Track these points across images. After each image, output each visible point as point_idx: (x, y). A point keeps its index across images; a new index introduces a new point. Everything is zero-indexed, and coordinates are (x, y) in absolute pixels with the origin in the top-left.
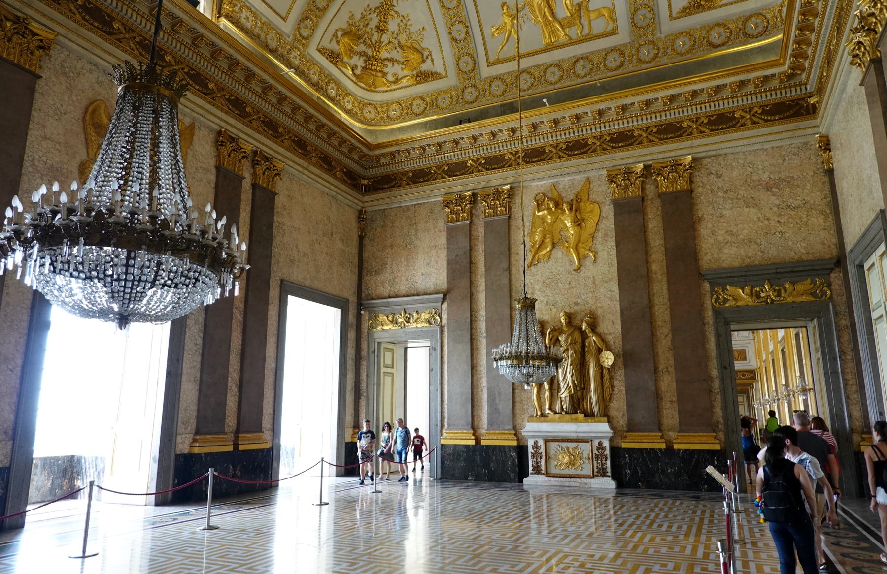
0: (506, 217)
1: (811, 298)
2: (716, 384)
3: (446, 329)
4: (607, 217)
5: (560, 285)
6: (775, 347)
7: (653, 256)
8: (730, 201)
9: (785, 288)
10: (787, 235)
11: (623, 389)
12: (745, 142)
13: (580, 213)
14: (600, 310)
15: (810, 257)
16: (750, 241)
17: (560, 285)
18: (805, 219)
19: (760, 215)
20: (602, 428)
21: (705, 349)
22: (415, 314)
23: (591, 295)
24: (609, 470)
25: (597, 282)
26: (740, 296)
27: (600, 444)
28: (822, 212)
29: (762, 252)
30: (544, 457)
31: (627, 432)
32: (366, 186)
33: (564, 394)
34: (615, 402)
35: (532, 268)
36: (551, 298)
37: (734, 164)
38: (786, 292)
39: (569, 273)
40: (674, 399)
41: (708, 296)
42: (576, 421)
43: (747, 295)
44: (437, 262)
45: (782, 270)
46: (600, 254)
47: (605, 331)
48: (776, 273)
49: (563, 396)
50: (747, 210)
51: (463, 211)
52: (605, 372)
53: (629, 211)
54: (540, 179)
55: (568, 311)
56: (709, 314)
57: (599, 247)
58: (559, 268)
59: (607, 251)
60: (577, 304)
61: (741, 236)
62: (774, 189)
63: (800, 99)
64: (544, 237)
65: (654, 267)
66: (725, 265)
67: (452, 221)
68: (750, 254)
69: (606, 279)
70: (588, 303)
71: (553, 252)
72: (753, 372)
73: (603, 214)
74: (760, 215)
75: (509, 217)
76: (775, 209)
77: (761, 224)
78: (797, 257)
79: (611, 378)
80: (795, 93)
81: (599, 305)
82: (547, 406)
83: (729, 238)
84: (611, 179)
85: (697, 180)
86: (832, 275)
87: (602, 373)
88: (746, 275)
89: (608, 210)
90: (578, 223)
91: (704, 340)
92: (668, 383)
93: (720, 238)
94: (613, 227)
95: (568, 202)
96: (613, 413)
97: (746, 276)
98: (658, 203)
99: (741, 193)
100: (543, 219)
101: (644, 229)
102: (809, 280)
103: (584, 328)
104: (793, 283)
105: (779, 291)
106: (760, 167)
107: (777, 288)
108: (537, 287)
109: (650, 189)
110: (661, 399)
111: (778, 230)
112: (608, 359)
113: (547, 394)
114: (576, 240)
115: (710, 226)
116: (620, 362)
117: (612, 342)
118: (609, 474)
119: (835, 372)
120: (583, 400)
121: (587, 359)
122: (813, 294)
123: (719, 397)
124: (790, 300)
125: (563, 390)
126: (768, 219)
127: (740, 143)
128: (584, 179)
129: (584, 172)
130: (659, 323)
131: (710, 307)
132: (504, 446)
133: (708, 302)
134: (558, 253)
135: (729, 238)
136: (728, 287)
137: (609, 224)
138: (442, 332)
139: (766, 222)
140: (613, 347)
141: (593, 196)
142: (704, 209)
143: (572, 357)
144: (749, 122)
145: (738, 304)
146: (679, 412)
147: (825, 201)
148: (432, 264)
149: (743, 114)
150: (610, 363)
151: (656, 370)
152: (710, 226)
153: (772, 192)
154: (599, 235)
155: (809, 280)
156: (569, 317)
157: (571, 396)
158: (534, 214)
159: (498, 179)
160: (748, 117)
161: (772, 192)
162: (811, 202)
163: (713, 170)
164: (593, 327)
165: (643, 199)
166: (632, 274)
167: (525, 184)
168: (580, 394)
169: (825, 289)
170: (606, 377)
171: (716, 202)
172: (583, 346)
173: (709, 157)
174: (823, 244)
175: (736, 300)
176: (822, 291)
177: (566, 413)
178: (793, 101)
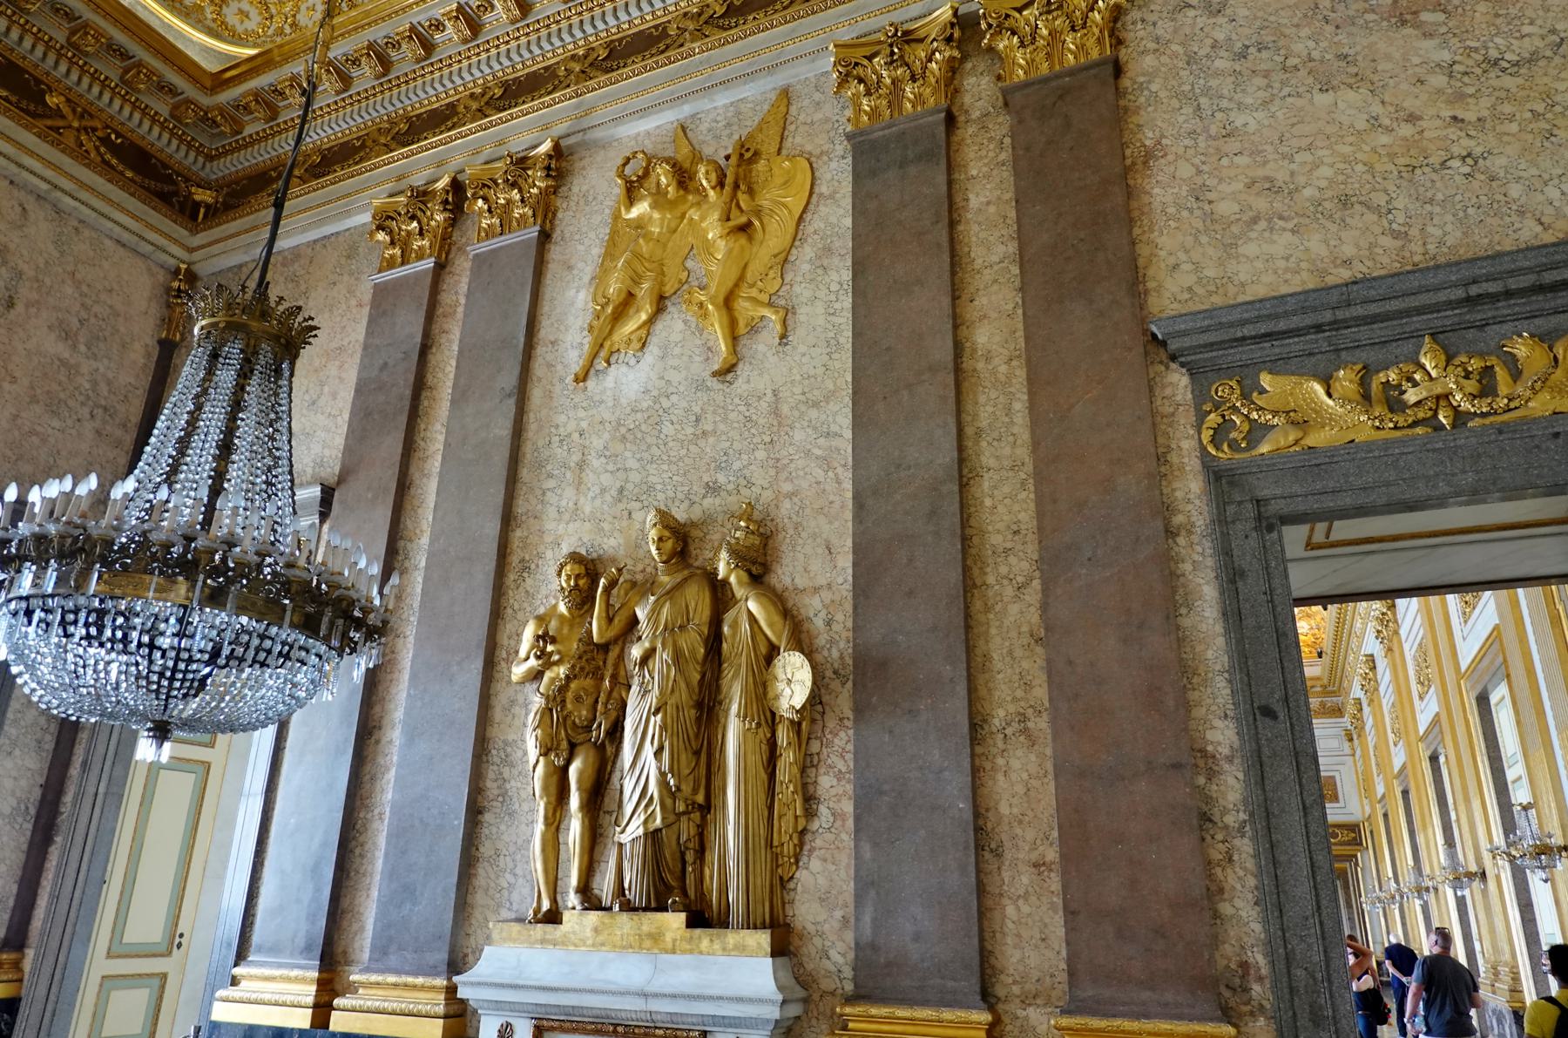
0: (533, 232)
2: (1231, 788)
4: (831, 197)
6: (1388, 787)
7: (982, 301)
8: (1259, 81)
9: (1512, 363)
10: (1497, 164)
11: (848, 807)
13: (751, 192)
14: (787, 504)
16: (1345, 202)
17: (668, 429)
19: (1377, 109)
21: (1180, 639)
23: (761, 454)
25: (785, 409)
26: (1319, 410)
29: (1396, 235)
31: (850, 1000)
32: (208, 206)
33: (631, 831)
34: (815, 864)
36: (635, 477)
38: (1516, 375)
39: (700, 386)
40: (1052, 854)
41: (1186, 419)
43: (1345, 400)
45: (1492, 287)
46: (802, 311)
47: (800, 582)
48: (1470, 301)
49: (625, 838)
50: (1323, 99)
52: (783, 736)
53: (905, 165)
54: (643, 112)
55: (680, 514)
57: (802, 291)
59: (824, 299)
60: (713, 489)
62: (1425, 16)
64: (636, 280)
65: (983, 337)
67: (390, 264)
68: (1348, 251)
69: (817, 394)
71: (659, 326)
72: (1353, 828)
73: (823, 188)
74: (1377, 109)
75: (545, 237)
76: (1439, 80)
77: (1385, 139)
79: (807, 765)
81: (787, 487)
82: (574, 881)
83: (1261, 204)
84: (849, 71)
87: (772, 744)
89: (838, 173)
91: (1170, 597)
92: (1024, 784)
93: (1226, 208)
94: (848, 222)
96: (806, 912)
97: (1336, 325)
98: (1001, 125)
99: (1299, 47)
100: (639, 225)
105: (1488, 371)
107: (1475, 364)
109: (978, 89)
111: (1457, 150)
112: (794, 682)
113: (575, 827)
114: (733, 275)
116: (843, 701)
117: (819, 622)
120: (701, 852)
121: (725, 682)
123: (1244, 847)
124: (1541, 405)
125: (628, 809)
126: (1412, 118)
129: (772, 69)
130: (996, 539)
131: (1193, 463)
133: (1186, 445)
134: (674, 324)
135: (1261, 204)
136: (1266, 380)
137: (836, 217)
139: (1406, 130)
140: (821, 641)
141: (796, 140)
142: (1161, 116)
143: (664, 678)
145: (1310, 441)
146: (1070, 913)
148: (322, 402)
150: (799, 700)
151: (977, 727)
152: (1185, 170)
153: (1417, 26)
154: (805, 255)
156: (681, 541)
157: (653, 837)
158: (617, 216)
159: (529, 129)
164: (758, 566)
165: (951, 120)
166: (906, 371)
167: (598, 134)
168: (687, 829)
170: (788, 757)
171: (1206, 91)
172: (714, 640)
175: (1302, 425)
177: (628, 907)
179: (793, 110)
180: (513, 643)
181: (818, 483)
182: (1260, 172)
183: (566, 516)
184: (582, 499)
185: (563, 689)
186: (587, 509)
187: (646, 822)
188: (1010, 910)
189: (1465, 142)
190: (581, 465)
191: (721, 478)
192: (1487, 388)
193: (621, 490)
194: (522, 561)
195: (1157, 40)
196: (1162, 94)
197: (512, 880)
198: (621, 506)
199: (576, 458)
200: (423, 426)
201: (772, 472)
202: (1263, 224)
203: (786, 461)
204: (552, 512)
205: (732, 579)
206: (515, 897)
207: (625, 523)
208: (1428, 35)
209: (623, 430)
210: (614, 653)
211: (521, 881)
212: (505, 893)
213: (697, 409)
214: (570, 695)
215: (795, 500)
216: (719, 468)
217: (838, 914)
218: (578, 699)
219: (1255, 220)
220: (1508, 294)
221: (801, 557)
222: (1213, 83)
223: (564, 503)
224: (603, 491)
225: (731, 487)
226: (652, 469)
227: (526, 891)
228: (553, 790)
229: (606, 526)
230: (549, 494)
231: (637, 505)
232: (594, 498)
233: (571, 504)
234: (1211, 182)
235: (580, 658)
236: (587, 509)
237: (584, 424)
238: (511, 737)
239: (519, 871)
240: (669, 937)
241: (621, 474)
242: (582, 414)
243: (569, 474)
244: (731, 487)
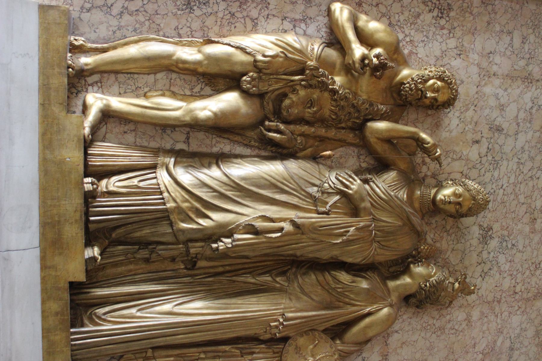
23: (507, 283)
70: (484, 275)
81: (475, 314)
181: (474, 346)
183: (485, 64)
184: (497, 82)
185: (323, 86)
186: (488, 90)
187: (179, 210)
191: (494, 244)
193: (499, 130)
197: (115, 11)
198: (485, 131)
203: (497, 309)
204: (490, 45)
205: (407, 280)
207: (470, 136)
210: (350, 137)
211: (114, 22)
214: (316, 94)
215: (464, 325)
216: (503, 239)
218: (311, 103)
221: (415, 337)
223: (497, 59)
226: (513, 165)
227: (103, 32)
228: (214, 70)
229: (470, 113)
231: (484, 150)
233: (495, 68)
235: (353, 106)
240: (58, 260)
243: (522, 63)
244: (485, 255)
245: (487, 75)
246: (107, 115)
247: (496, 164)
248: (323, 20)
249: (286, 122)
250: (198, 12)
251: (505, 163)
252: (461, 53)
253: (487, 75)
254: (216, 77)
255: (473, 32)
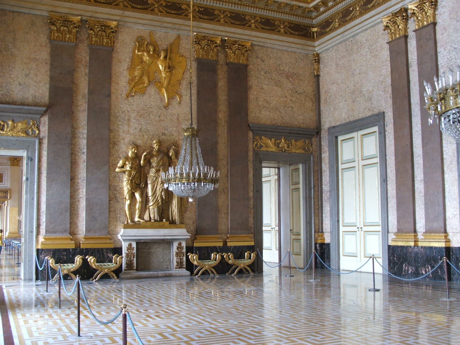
1: (303, 152)
2: (251, 202)
3: (45, 141)
5: (152, 117)
7: (220, 107)
8: (267, 79)
9: (292, 143)
10: (295, 110)
12: (280, 43)
15: (304, 126)
16: (276, 109)
17: (152, 117)
18: (303, 102)
19: (282, 94)
20: (181, 233)
22: (10, 123)
23: (175, 129)
24: (185, 263)
25: (180, 119)
27: (180, 244)
28: (312, 99)
30: (135, 257)
34: (188, 213)
35: (130, 99)
36: (144, 127)
37: (271, 55)
38: (292, 145)
42: (163, 227)
44: (36, 75)
48: (289, 133)
50: (276, 88)
51: (70, 32)
53: (206, 68)
56: (251, 154)
58: (152, 103)
60: (164, 134)
61: (272, 105)
62: (290, 79)
63: (308, 26)
66: (262, 122)
68: (276, 118)
70: (173, 135)
74: (282, 94)
76: (290, 92)
77: (282, 99)
78: (298, 125)
80: (306, 21)
83: (265, 104)
84: (198, 41)
85: (250, 59)
86: (313, 139)
88: (275, 131)
90: (170, 68)
91: (247, 173)
93: (260, 103)
95: (163, 50)
97: (274, 132)
98: (225, 68)
101: (215, 85)
102: (303, 141)
103: (171, 154)
104: (296, 141)
106: (284, 62)
107: (288, 143)
108: (133, 115)
110: (219, 211)
111: (291, 106)
115: (255, 93)
118: (185, 266)
119: (310, 197)
122: (304, 149)
124: (294, 151)
126: (286, 97)
127: (277, 42)
128: (176, 36)
129: (178, 29)
130: (221, 157)
131: (251, 149)
132: (102, 249)
133: (251, 146)
135: (265, 104)
136: (263, 137)
138: (40, 143)
139: (285, 99)
141: (182, 51)
142: (253, 82)
144: (282, 30)
147: (313, 93)
148: (31, 75)
149: (219, 13)
152: (255, 93)
153: (289, 80)
154: (185, 83)
155: (303, 141)
160: (222, 16)
161: (289, 80)
162: (307, 92)
163: (260, 55)
169: (310, 147)
171: (260, 78)
173: (258, 46)
174: (310, 119)
175: (267, 147)
176: (308, 147)
178: (304, 26)
179: (181, 42)
180: (113, 162)
182: (266, 98)
183: (126, 133)
184: (130, 130)
188: (220, 220)
189: (292, 105)
190: (129, 120)
191: (166, 132)
192: (288, 147)
193: (141, 129)
194: (114, 141)
195: (253, 62)
196: (253, 75)
197: (120, 216)
198: (141, 133)
199: (127, 118)
200: (75, 96)
201: (178, 133)
202: (265, 109)
204: (121, 131)
206: (121, 219)
208: (290, 83)
209: (140, 114)
212: (119, 218)
213: (159, 114)
214: (136, 177)
216: (165, 130)
217: (192, 221)
219: (264, 107)
220: (293, 133)
222: (261, 77)
224: (136, 128)
225: (168, 135)
226: (148, 125)
227: (124, 218)
230: (120, 126)
232: (133, 130)
233: (127, 130)
234: (259, 97)
236: (132, 132)
237: (129, 109)
238: (116, 184)
239: (121, 214)
241: (140, 125)
242: (128, 106)
243: (125, 122)
244: (168, 135)
245: (128, 132)
246: (139, 217)
247: (148, 130)
248: (119, 174)
249: (141, 183)
250: (119, 200)
251: (148, 128)
252: (124, 139)
253: (128, 132)
254: (132, 197)
255: (119, 135)
